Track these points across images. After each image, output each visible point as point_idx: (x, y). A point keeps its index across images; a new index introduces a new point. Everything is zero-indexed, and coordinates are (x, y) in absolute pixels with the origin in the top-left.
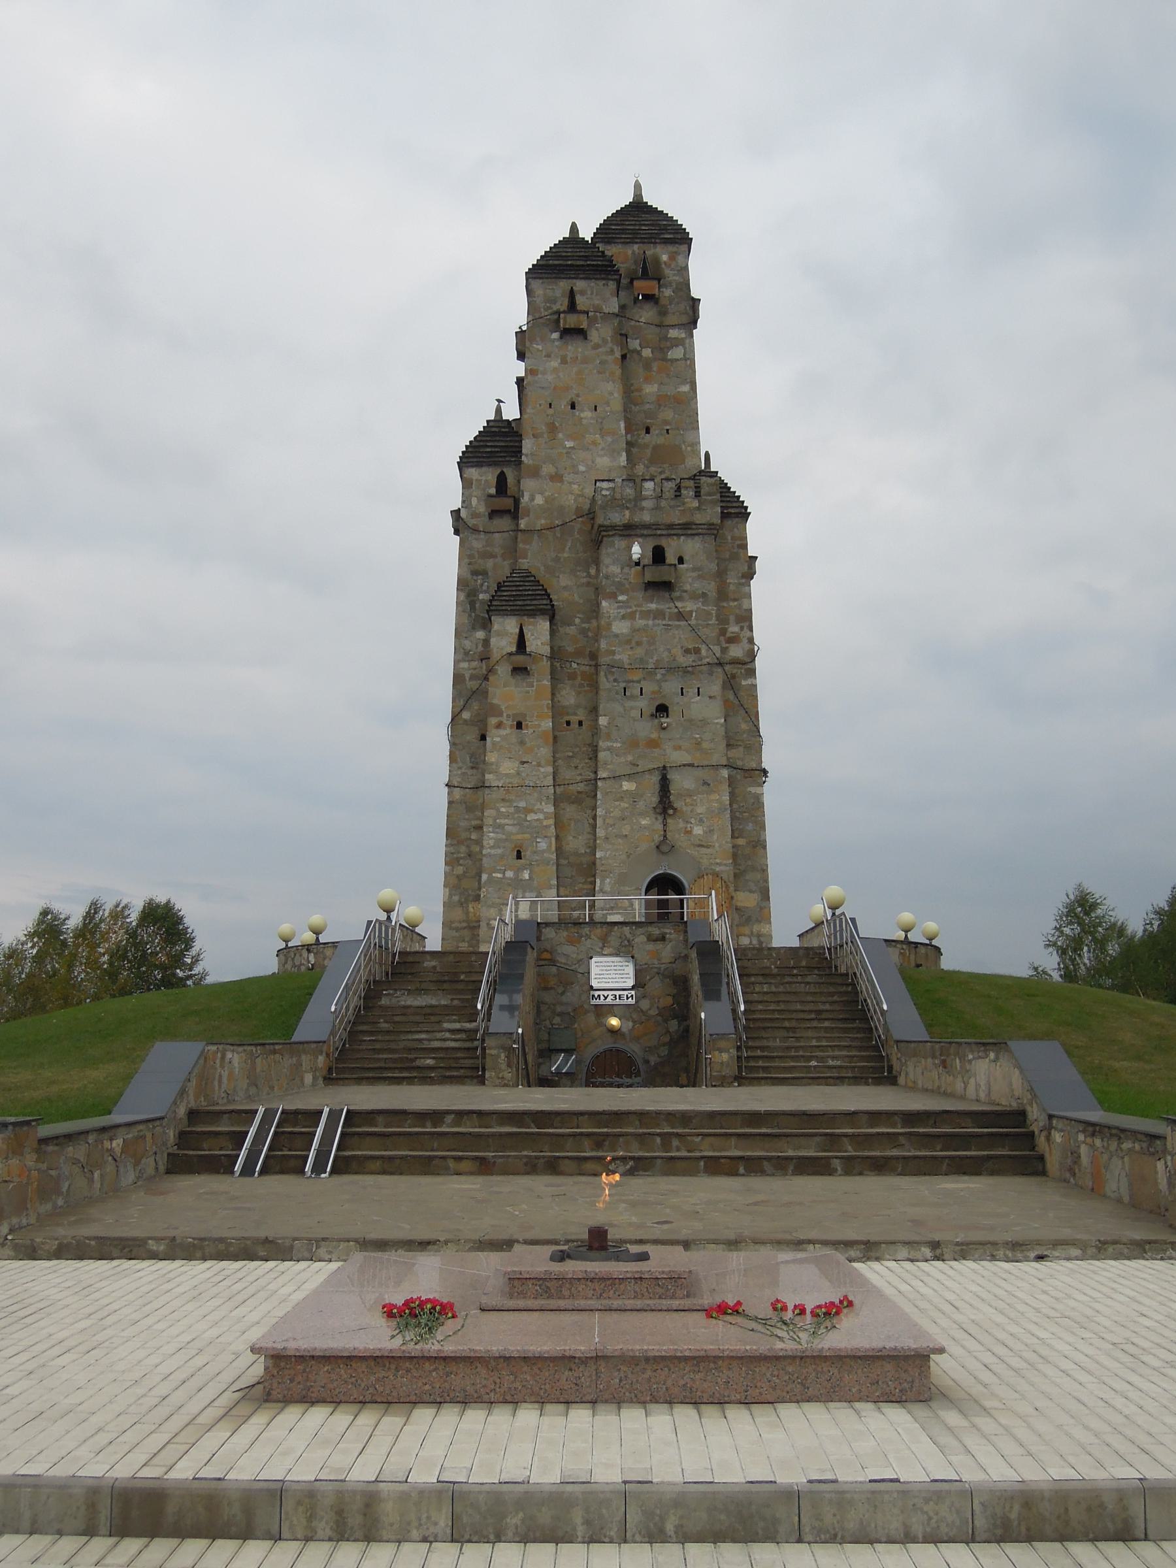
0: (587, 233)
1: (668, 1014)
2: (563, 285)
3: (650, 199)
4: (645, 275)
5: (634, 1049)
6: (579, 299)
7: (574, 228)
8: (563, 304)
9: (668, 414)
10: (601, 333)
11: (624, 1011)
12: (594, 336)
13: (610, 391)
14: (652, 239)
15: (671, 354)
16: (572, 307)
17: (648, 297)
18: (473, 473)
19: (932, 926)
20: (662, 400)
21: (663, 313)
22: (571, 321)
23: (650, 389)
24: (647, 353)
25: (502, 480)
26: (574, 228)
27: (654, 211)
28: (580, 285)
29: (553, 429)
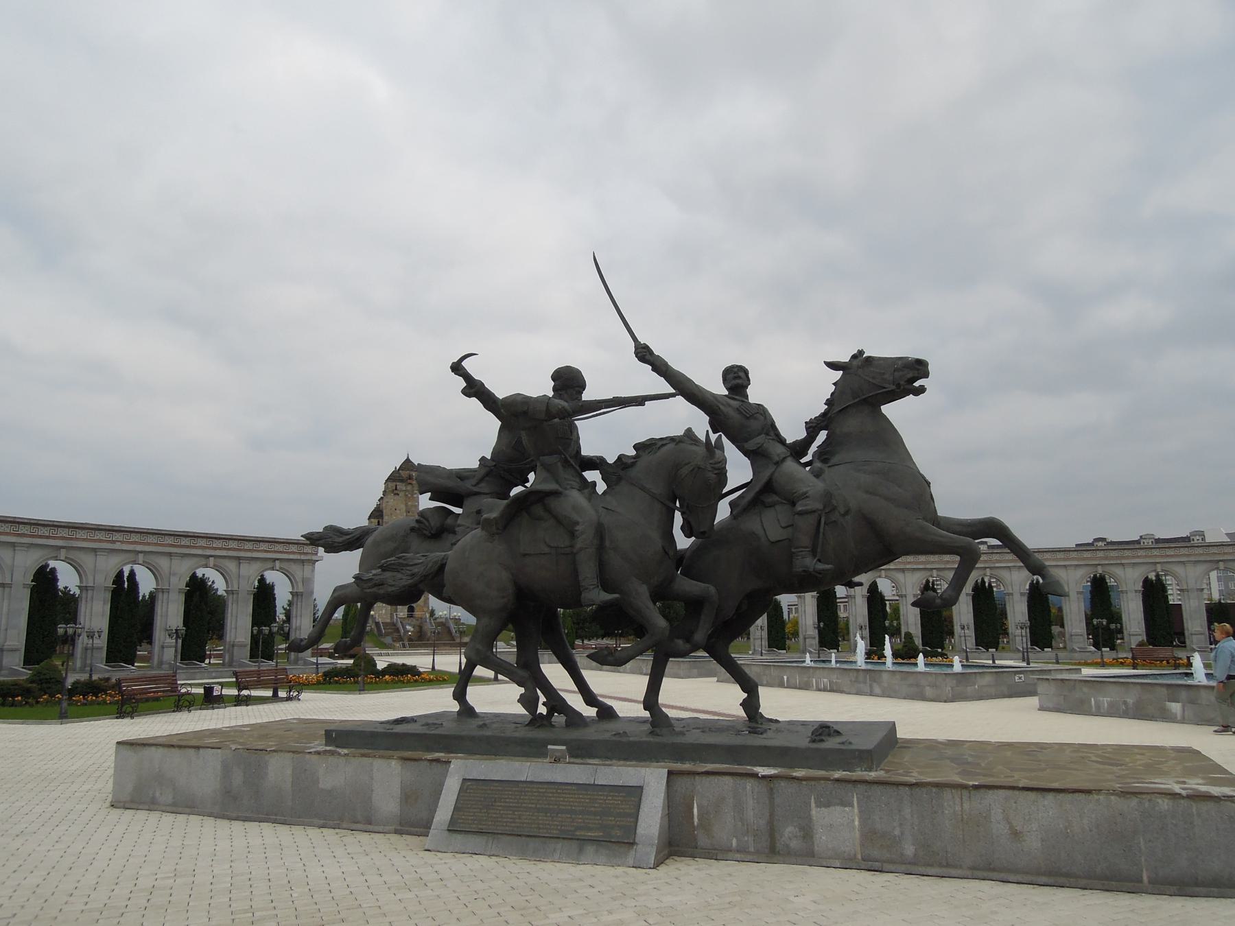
0: (398, 468)
1: (418, 632)
2: (395, 483)
3: (410, 458)
4: (410, 479)
5: (413, 638)
6: (398, 487)
7: (396, 468)
8: (394, 488)
9: (413, 509)
10: (401, 494)
11: (412, 632)
12: (400, 495)
13: (403, 507)
14: (412, 470)
15: (415, 496)
16: (396, 489)
17: (410, 484)
18: (372, 520)
19: (459, 614)
20: (412, 506)
21: (413, 487)
22: (396, 492)
23: (409, 503)
24: (409, 495)
25: (379, 522)
26: (396, 468)
27: (411, 462)
28: (398, 483)
29: (391, 514)
